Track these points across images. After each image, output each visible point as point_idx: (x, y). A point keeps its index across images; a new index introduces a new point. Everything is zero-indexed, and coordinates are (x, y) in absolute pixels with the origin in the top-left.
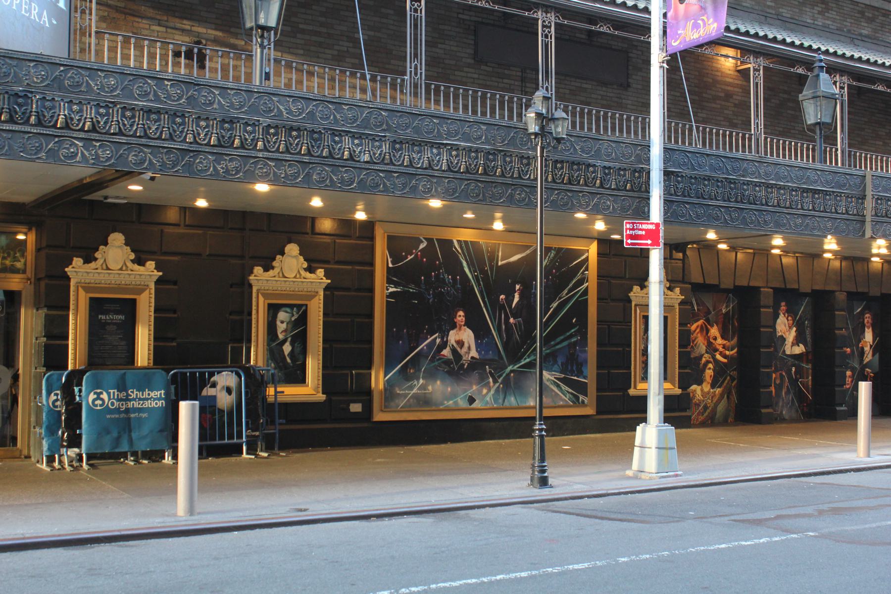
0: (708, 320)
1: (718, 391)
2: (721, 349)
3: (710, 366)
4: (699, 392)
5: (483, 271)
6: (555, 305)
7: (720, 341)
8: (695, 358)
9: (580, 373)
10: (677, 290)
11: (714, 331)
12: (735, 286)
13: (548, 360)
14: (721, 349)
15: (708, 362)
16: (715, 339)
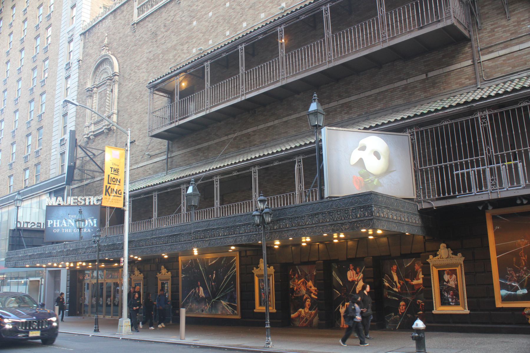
0: (306, 279)
1: (313, 312)
2: (314, 292)
3: (308, 300)
4: (303, 312)
5: (205, 268)
6: (226, 277)
7: (313, 288)
8: (301, 296)
9: (235, 303)
10: (272, 267)
11: (310, 283)
12: (347, 259)
13: (223, 298)
14: (314, 292)
15: (307, 298)
16: (311, 287)
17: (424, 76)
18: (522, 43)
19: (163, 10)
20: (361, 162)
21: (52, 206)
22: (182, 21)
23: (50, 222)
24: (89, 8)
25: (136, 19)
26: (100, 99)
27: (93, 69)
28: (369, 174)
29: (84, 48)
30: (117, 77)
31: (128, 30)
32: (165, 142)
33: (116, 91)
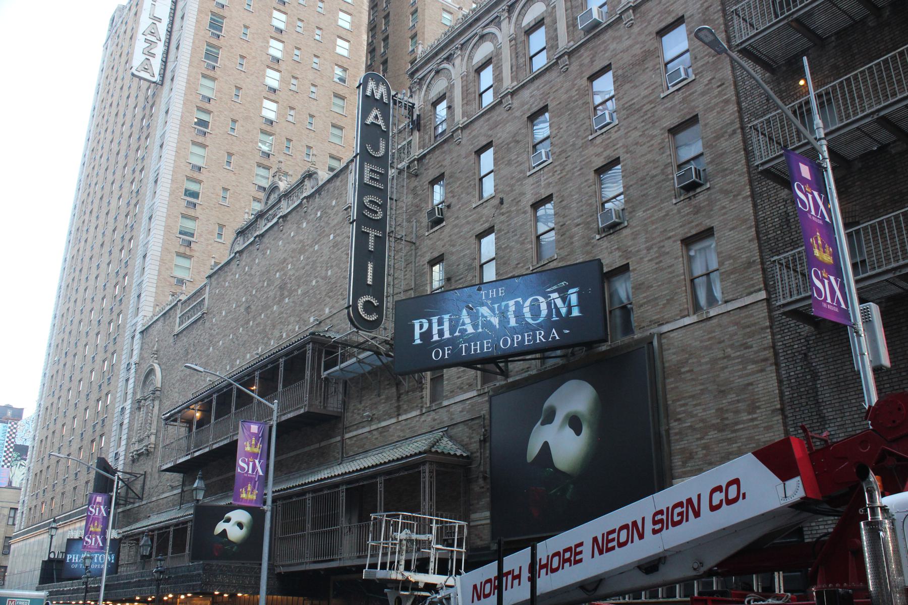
17: (317, 446)
18: (363, 427)
19: (195, 326)
20: (224, 532)
21: (74, 540)
22: (204, 344)
23: (69, 557)
24: (152, 299)
25: (177, 329)
26: (147, 413)
27: (142, 378)
28: (230, 542)
29: (141, 349)
30: (158, 393)
31: (172, 340)
32: (182, 475)
33: (156, 408)
